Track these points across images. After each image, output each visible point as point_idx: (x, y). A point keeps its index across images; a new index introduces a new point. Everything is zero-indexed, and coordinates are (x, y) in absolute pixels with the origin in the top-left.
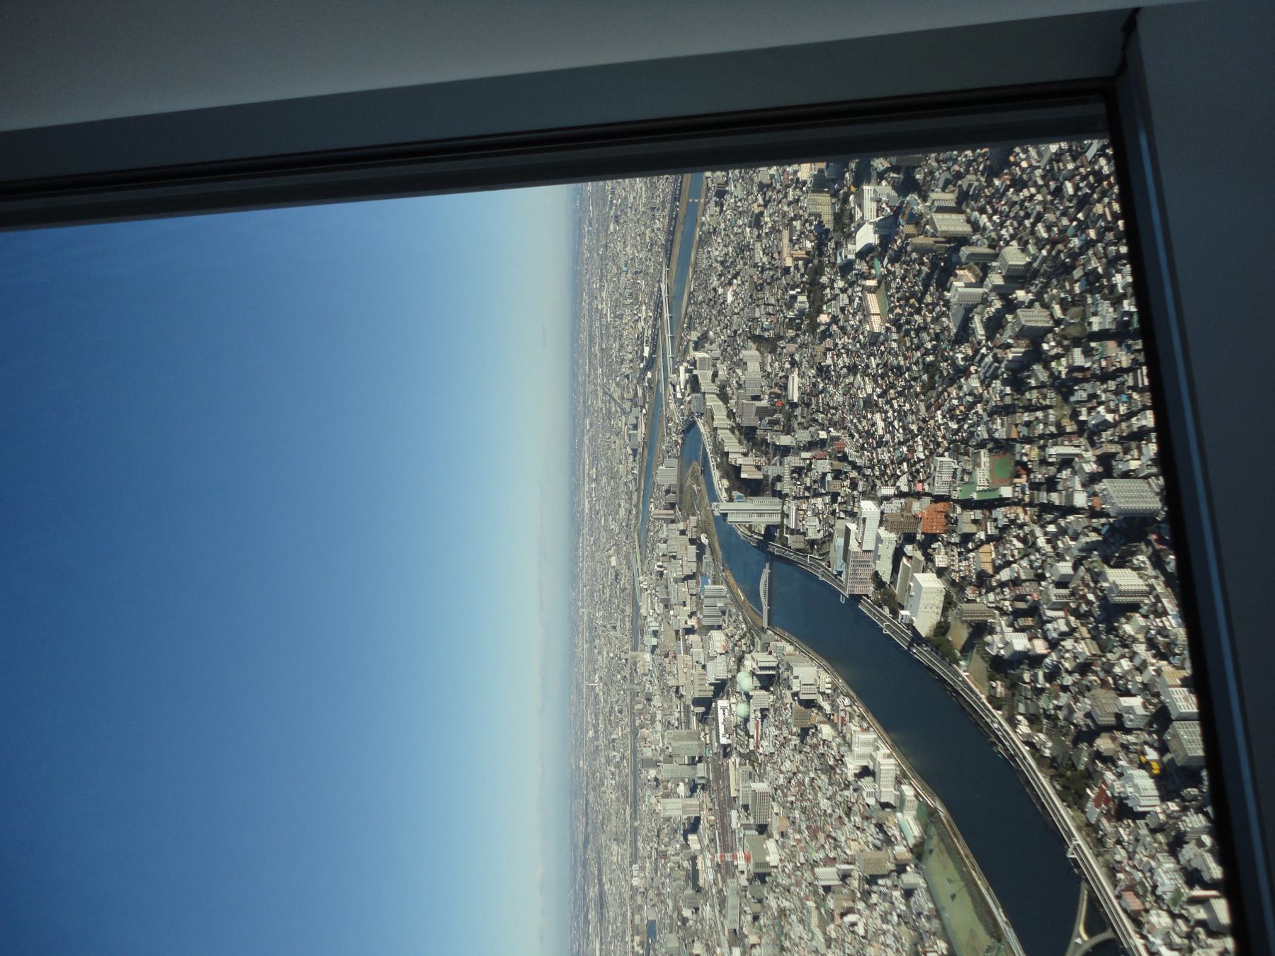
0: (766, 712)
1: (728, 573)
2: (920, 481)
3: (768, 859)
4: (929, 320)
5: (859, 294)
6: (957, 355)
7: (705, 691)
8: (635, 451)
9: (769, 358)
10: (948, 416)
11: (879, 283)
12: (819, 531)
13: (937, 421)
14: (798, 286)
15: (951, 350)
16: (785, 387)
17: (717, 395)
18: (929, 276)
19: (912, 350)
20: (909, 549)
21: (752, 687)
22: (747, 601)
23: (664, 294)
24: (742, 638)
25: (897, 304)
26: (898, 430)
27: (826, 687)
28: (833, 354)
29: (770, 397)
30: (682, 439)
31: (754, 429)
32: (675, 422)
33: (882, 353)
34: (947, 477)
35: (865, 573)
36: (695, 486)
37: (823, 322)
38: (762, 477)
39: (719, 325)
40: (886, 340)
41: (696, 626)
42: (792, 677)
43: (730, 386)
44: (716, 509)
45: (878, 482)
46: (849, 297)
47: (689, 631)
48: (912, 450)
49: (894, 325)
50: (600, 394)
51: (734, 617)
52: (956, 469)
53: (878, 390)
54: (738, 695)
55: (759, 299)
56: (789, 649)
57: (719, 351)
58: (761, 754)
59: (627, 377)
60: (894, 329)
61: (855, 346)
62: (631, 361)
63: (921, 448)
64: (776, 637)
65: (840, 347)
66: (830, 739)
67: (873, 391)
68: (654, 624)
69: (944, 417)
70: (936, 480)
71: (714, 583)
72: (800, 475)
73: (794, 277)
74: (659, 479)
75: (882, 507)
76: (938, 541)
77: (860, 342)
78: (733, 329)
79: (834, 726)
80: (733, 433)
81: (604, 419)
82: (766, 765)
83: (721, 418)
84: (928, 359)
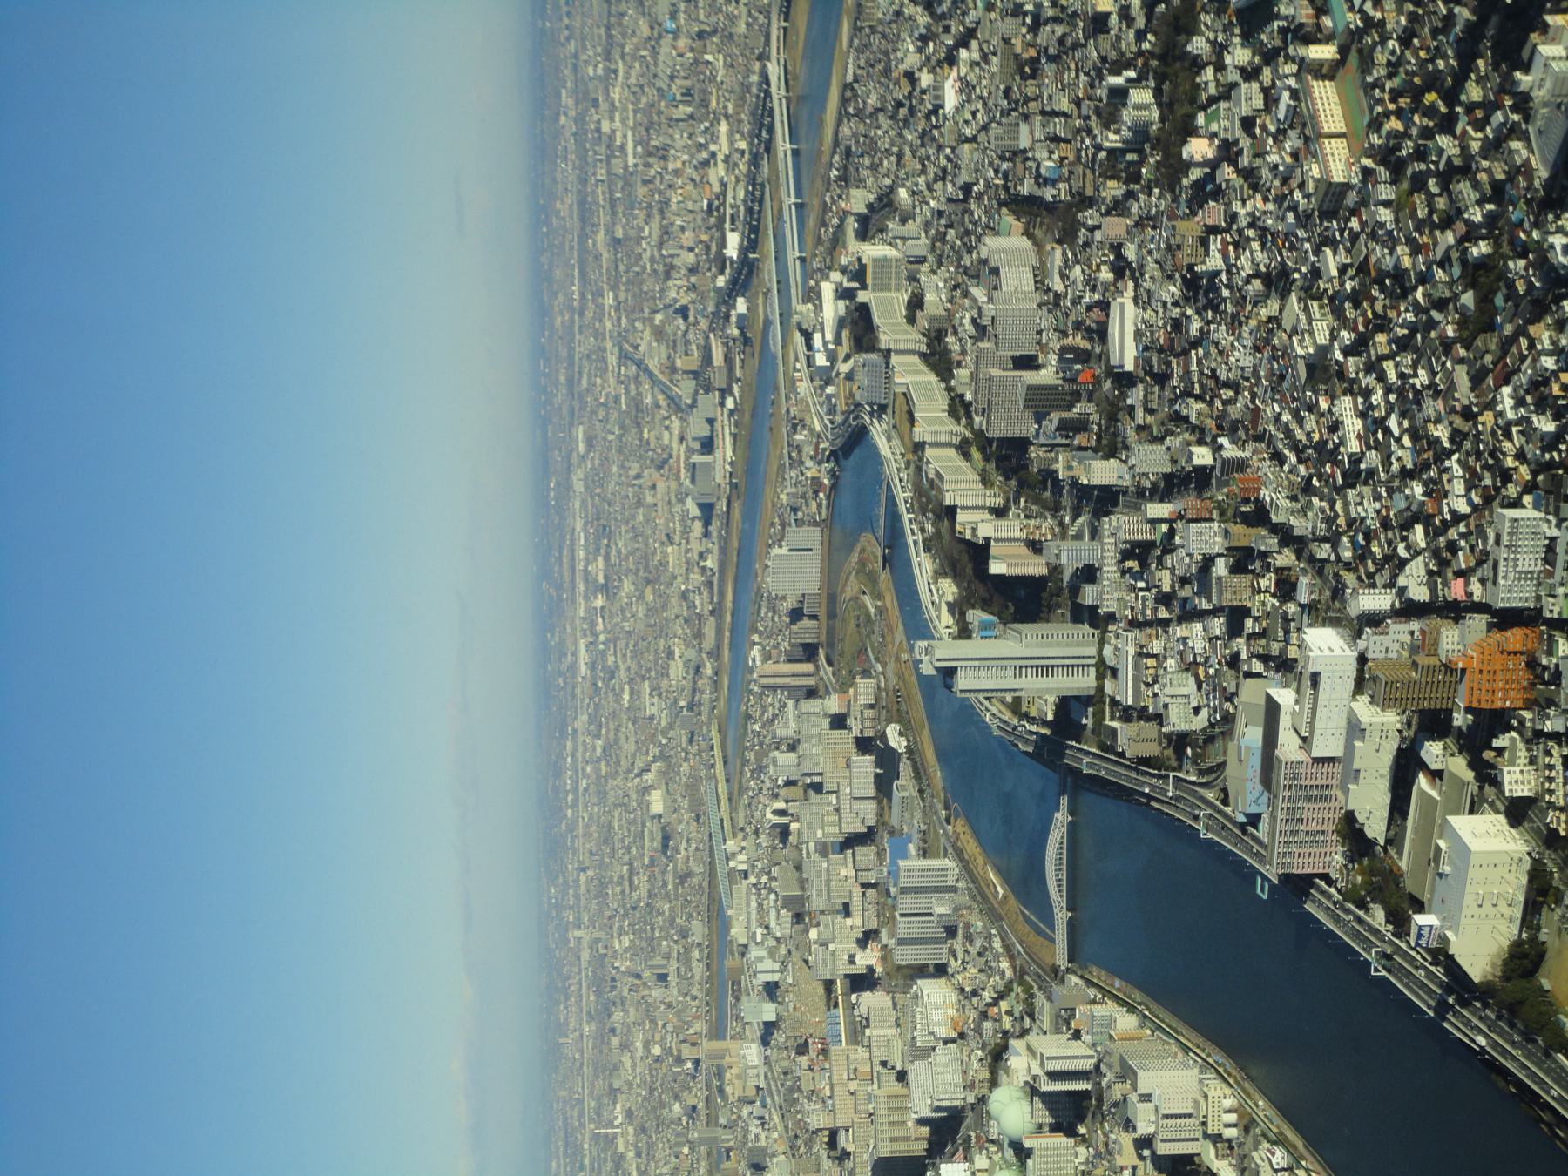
1: (960, 826)
2: (1459, 574)
4: (1475, 146)
5: (1292, 82)
6: (1551, 239)
7: (907, 1139)
8: (707, 510)
9: (1057, 256)
10: (1529, 399)
11: (1344, 51)
13: (1501, 414)
14: (1129, 65)
15: (1536, 225)
16: (1101, 333)
17: (922, 355)
18: (1474, 32)
19: (1433, 226)
20: (1433, 752)
21: (1030, 1127)
22: (1013, 901)
23: (777, 91)
24: (1001, 996)
25: (1391, 107)
26: (1398, 440)
27: (1225, 1122)
28: (1225, 244)
29: (1061, 359)
30: (832, 473)
31: (1022, 444)
32: (812, 430)
33: (1354, 237)
34: (1530, 561)
35: (1322, 819)
36: (867, 600)
37: (1198, 158)
38: (1044, 571)
39: (923, 171)
40: (1364, 202)
41: (879, 969)
42: (1134, 1097)
43: (955, 333)
44: (926, 659)
45: (1349, 578)
46: (1265, 91)
47: (862, 982)
48: (1436, 491)
49: (1383, 162)
50: (612, 360)
51: (978, 943)
52: (1553, 539)
53: (1345, 334)
54: (993, 1148)
55: (1027, 100)
56: (1126, 1022)
57: (924, 241)
59: (683, 312)
60: (1383, 173)
61: (1283, 219)
62: (693, 270)
63: (1459, 487)
64: (1092, 992)
65: (1243, 222)
67: (1333, 338)
68: (769, 965)
69: (1520, 402)
70: (1501, 568)
71: (925, 853)
72: (1144, 565)
73: (1119, 38)
74: (772, 583)
75: (1362, 644)
76: (1509, 728)
77: (1294, 208)
78: (960, 182)
80: (966, 456)
81: (622, 427)
83: (933, 419)
84: (1475, 251)
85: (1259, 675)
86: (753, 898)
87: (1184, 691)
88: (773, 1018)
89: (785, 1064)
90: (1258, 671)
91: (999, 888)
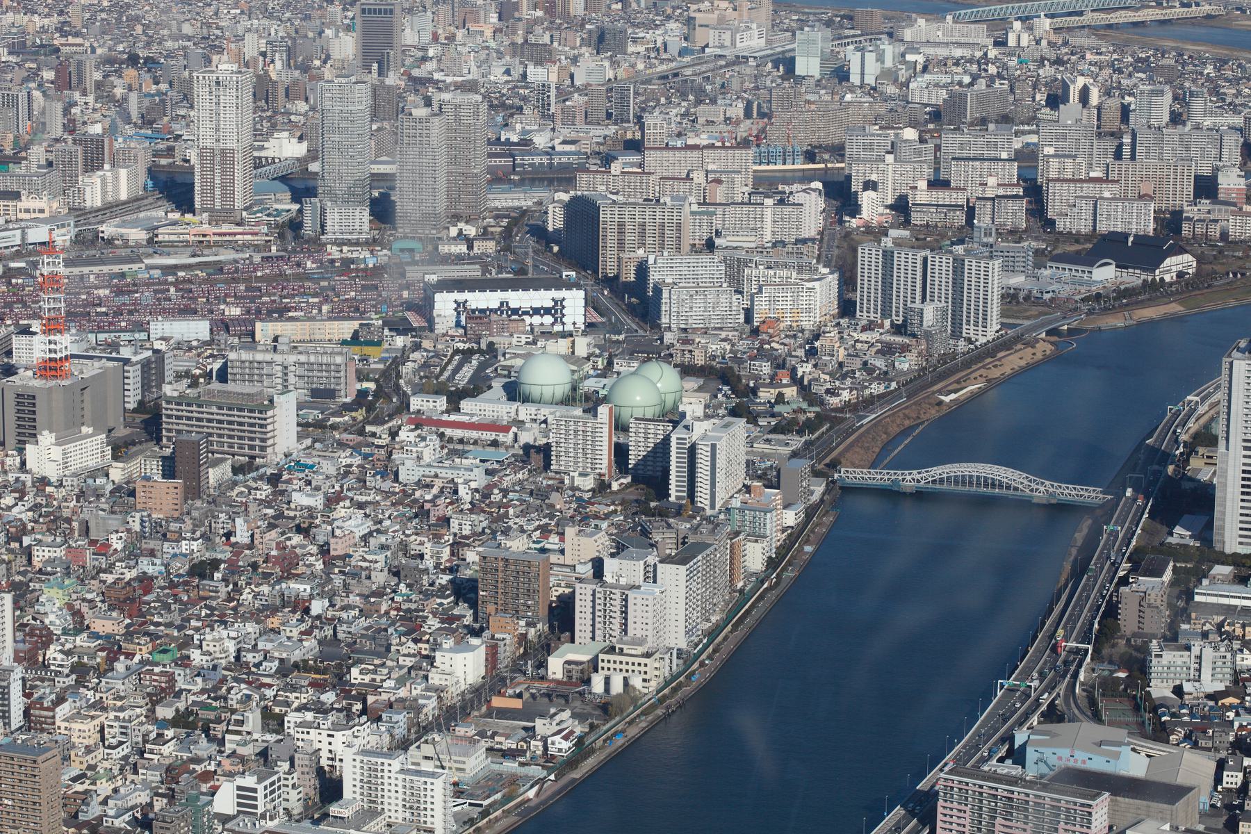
0: (536, 460)
1: (1044, 348)
3: (46, 438)
7: (621, 245)
12: (1178, 691)
21: (625, 414)
22: (933, 413)
24: (804, 389)
41: (854, 223)
42: (652, 559)
51: (880, 363)
54: (601, 364)
56: (755, 557)
58: (394, 434)
66: (435, 679)
68: (872, 69)
71: (1010, 298)
79: (478, 696)
82: (356, 448)
85: (1218, 779)
86: (967, 53)
87: (1206, 674)
88: (800, 70)
89: (735, 84)
90: (1225, 779)
91: (953, 396)
